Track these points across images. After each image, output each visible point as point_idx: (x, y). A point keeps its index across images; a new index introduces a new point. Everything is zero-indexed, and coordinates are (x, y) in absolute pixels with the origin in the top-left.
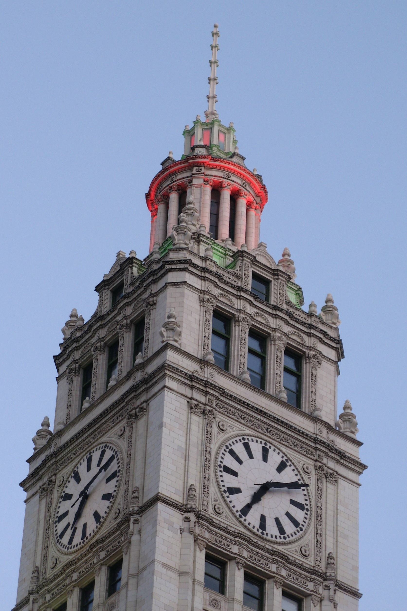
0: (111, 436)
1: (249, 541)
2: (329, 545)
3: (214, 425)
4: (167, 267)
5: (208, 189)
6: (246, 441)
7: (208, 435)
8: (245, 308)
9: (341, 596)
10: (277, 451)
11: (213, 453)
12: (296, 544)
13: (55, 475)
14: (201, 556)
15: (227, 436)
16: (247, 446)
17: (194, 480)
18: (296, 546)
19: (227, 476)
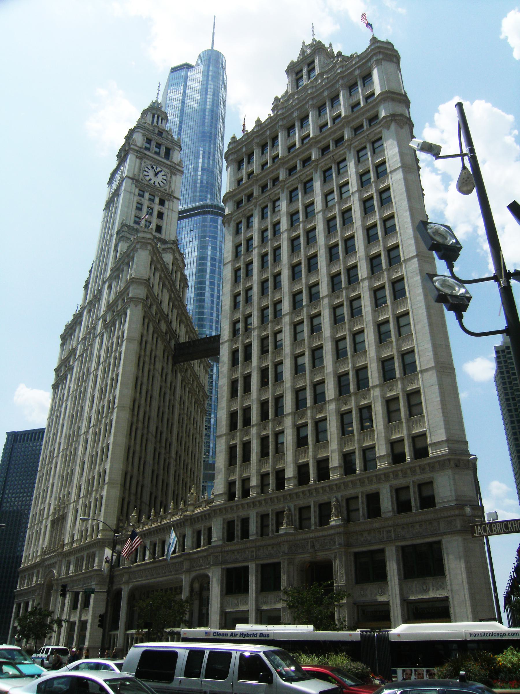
2: (173, 188)
3: (143, 162)
5: (152, 115)
7: (141, 164)
8: (155, 137)
9: (175, 200)
14: (137, 190)
17: (136, 173)
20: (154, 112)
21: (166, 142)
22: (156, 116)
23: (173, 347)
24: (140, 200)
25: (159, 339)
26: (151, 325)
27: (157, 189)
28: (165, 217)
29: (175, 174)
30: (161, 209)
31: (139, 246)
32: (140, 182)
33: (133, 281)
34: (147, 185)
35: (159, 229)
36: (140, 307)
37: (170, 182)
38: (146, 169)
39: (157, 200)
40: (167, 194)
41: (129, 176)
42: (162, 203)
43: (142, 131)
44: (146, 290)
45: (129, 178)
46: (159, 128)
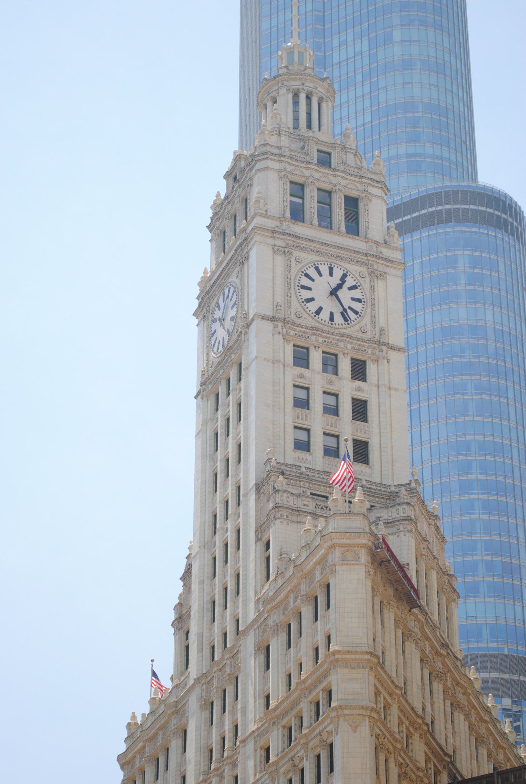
0: (233, 278)
1: (322, 331)
2: (382, 322)
3: (293, 260)
4: (256, 159)
5: (290, 96)
6: (317, 265)
7: (288, 268)
10: (339, 267)
11: (293, 278)
12: (357, 326)
13: (209, 306)
15: (302, 264)
16: (317, 269)
17: (280, 298)
18: (357, 327)
21: (344, 182)
24: (301, 376)
26: (392, 764)
28: (372, 412)
29: (382, 276)
30: (359, 389)
32: (294, 324)
33: (337, 660)
34: (313, 328)
35: (361, 451)
36: (365, 729)
37: (373, 305)
38: (305, 282)
39: (345, 366)
40: (369, 341)
41: (263, 312)
42: (359, 370)
43: (276, 165)
44: (372, 678)
45: (264, 318)
46: (318, 142)
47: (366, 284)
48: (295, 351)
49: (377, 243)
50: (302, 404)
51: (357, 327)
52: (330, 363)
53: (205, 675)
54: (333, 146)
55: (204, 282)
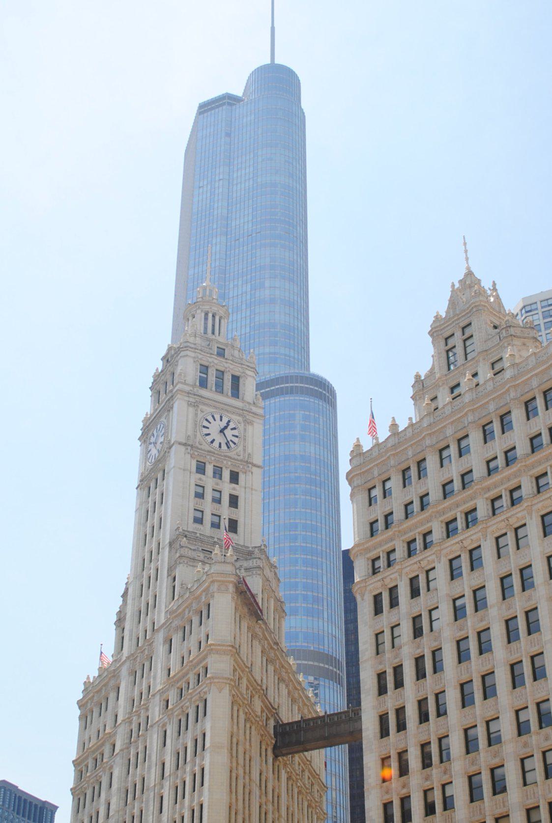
0: (163, 419)
2: (249, 450)
5: (203, 314)
7: (196, 415)
16: (213, 416)
18: (235, 452)
19: (204, 429)
20: (206, 308)
21: (231, 367)
22: (210, 315)
23: (272, 732)
24: (200, 479)
25: (253, 728)
26: (241, 713)
27: (225, 456)
29: (251, 423)
30: (234, 489)
31: (214, 587)
32: (197, 448)
34: (209, 451)
35: (233, 526)
36: (226, 691)
37: (245, 439)
38: (206, 424)
39: (226, 475)
40: (241, 461)
41: (180, 440)
42: (234, 478)
43: (193, 355)
44: (233, 662)
45: (180, 444)
46: (218, 342)
47: (241, 427)
48: (197, 465)
49: (249, 403)
50: (200, 496)
51: (235, 452)
52: (218, 473)
53: (132, 655)
54: (226, 345)
55: (146, 420)
